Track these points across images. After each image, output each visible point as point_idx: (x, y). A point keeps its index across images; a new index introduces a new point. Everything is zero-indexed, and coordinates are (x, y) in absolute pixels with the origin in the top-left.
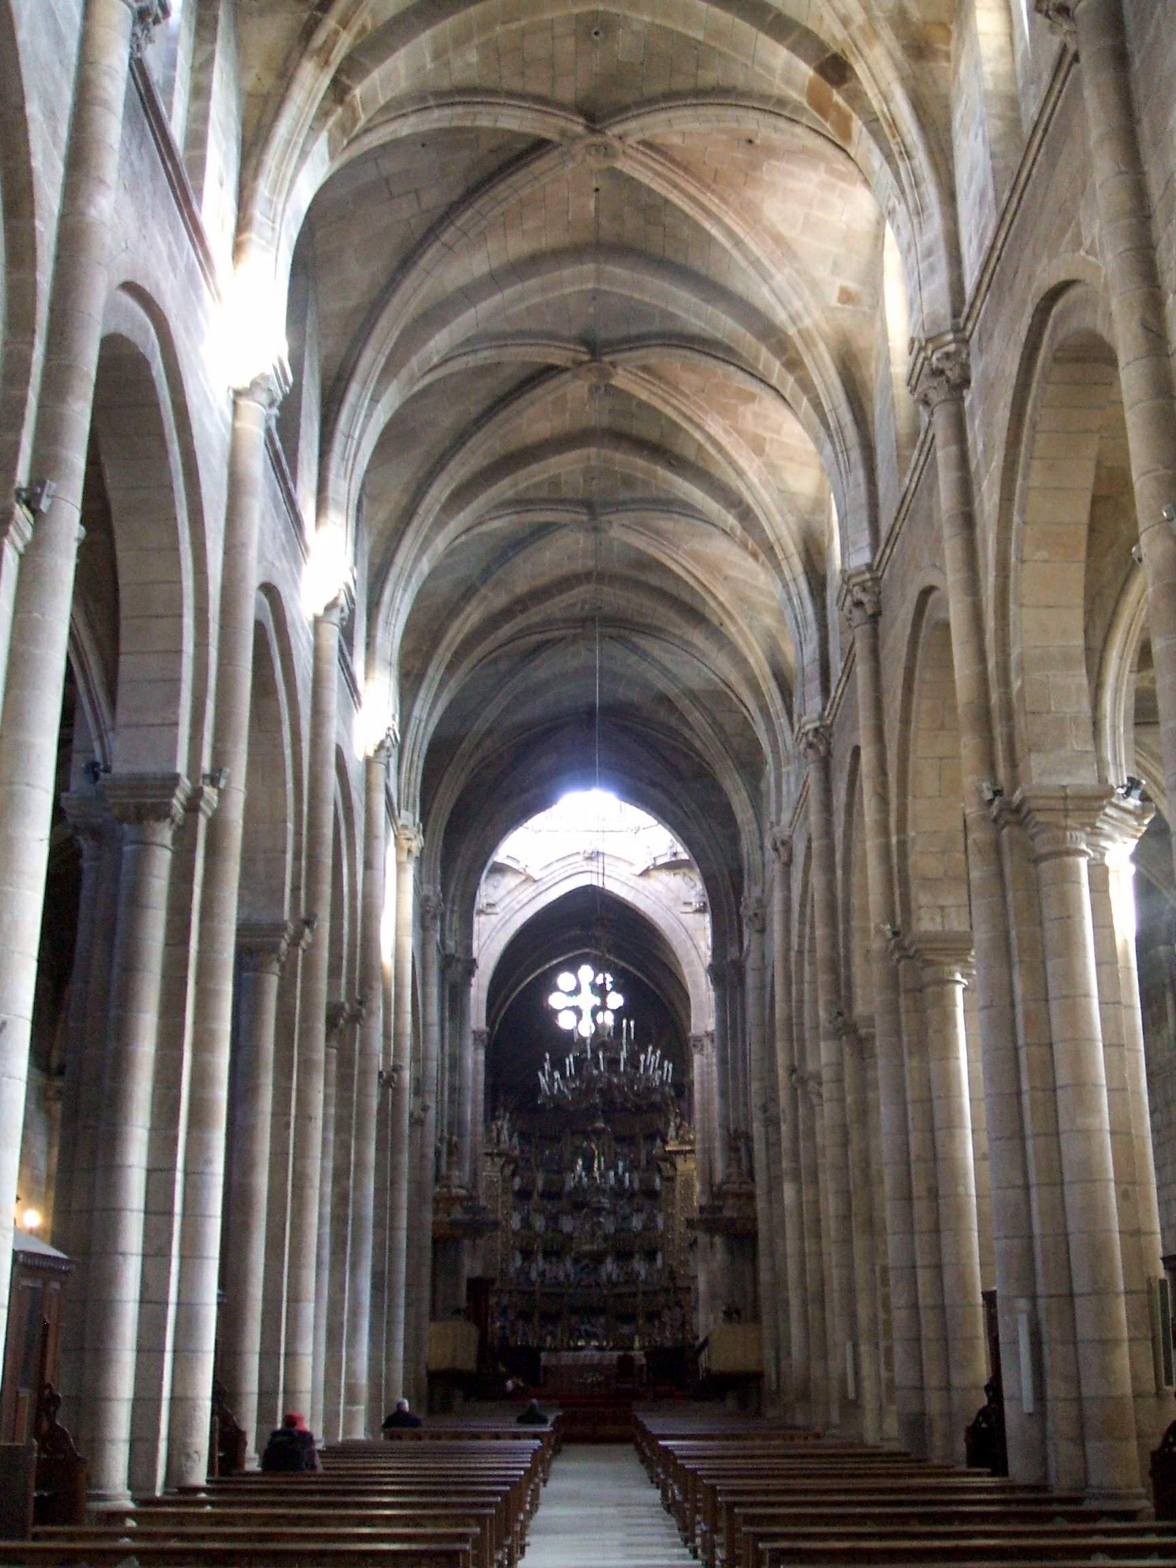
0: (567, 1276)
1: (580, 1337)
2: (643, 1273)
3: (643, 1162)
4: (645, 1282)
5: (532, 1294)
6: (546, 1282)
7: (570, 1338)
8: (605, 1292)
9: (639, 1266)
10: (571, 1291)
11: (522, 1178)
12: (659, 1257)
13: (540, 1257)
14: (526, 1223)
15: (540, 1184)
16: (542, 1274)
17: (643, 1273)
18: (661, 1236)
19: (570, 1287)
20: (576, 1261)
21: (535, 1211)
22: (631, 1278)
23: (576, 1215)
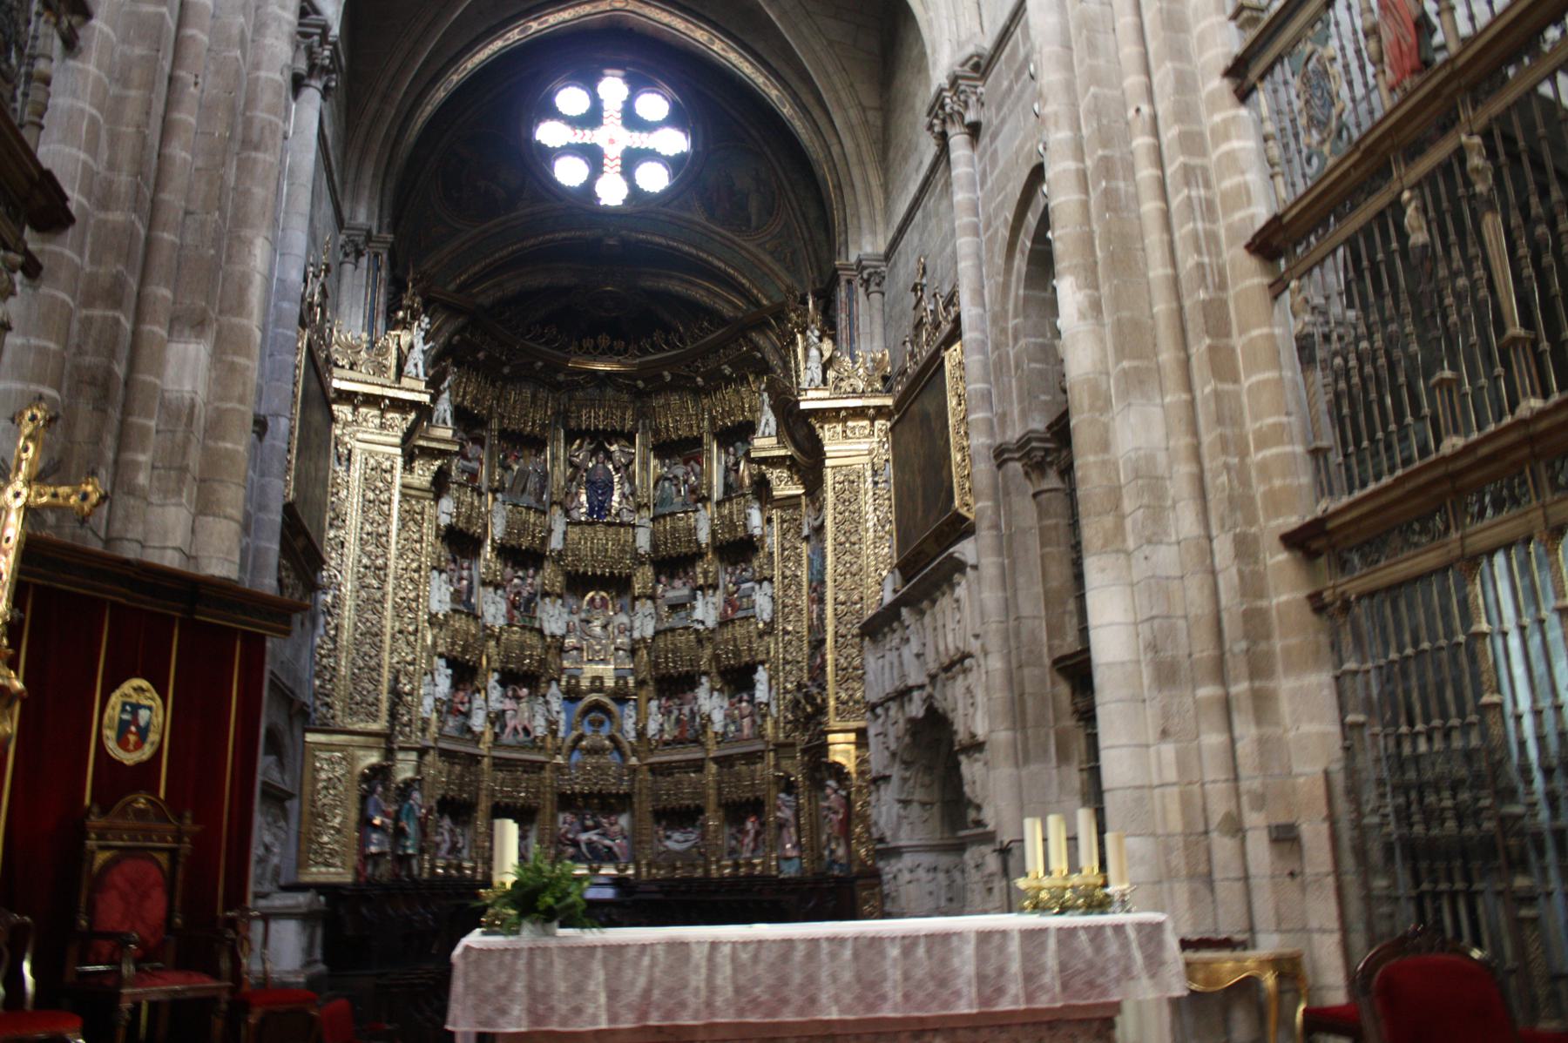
0: (552, 725)
1: (576, 859)
2: (718, 717)
4: (722, 738)
5: (474, 759)
6: (507, 738)
8: (633, 761)
9: (711, 703)
10: (559, 759)
11: (459, 504)
12: (761, 675)
14: (463, 603)
15: (497, 530)
16: (497, 718)
17: (718, 717)
18: (770, 628)
19: (558, 750)
20: (572, 695)
21: (484, 583)
22: (692, 731)
23: (571, 601)
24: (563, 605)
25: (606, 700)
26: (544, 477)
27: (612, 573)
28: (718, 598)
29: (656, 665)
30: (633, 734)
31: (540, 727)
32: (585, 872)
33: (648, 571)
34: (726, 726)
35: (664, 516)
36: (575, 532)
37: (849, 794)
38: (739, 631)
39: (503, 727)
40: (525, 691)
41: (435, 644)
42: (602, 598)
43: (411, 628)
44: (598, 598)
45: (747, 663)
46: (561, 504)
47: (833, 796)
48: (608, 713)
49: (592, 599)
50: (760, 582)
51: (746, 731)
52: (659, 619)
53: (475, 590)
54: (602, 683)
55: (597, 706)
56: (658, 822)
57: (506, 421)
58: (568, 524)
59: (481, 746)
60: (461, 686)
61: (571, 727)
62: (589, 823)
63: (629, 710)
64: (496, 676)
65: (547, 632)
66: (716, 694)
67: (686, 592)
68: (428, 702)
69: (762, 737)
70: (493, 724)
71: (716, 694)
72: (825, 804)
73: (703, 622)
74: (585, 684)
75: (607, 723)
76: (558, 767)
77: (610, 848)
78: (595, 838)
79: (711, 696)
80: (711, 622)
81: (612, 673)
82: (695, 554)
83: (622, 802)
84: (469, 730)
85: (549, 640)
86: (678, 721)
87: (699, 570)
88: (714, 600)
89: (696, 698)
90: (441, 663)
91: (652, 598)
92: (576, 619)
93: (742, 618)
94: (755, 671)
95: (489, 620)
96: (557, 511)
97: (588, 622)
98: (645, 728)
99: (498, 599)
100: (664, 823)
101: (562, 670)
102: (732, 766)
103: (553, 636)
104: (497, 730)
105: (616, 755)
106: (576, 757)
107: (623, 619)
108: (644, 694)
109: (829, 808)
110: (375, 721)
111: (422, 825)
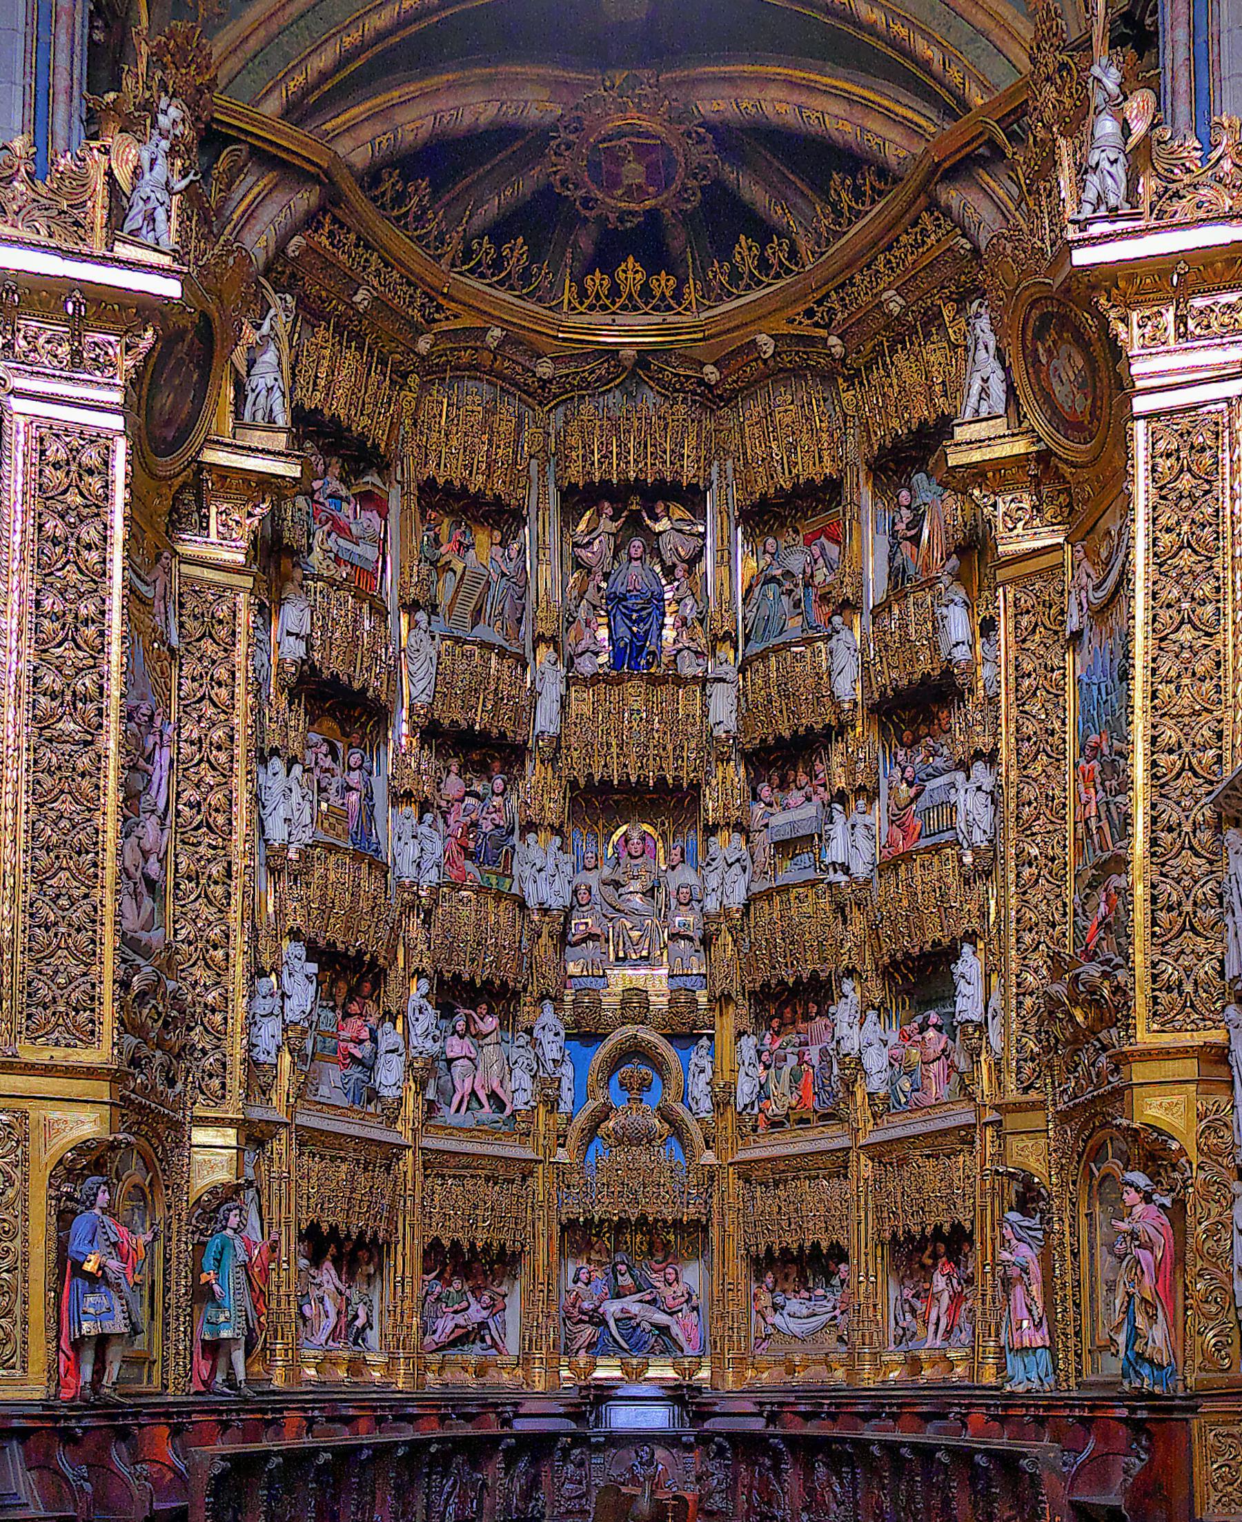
4: (882, 1107)
8: (709, 1157)
12: (970, 964)
13: (418, 989)
17: (875, 1060)
19: (561, 1139)
21: (399, 798)
25: (648, 1035)
26: (520, 584)
30: (706, 1104)
32: (618, 1373)
33: (735, 774)
34: (892, 1083)
35: (763, 656)
36: (582, 703)
40: (491, 1023)
42: (644, 837)
43: (216, 870)
44: (635, 835)
46: (553, 641)
48: (659, 1066)
49: (626, 838)
50: (964, 766)
53: (378, 812)
55: (634, 1052)
56: (759, 1278)
57: (432, 465)
59: (399, 1127)
60: (354, 1008)
62: (626, 1280)
63: (699, 1057)
64: (424, 985)
65: (531, 903)
66: (872, 1015)
67: (811, 810)
70: (422, 1085)
71: (872, 1015)
72: (1124, 1226)
75: (657, 1081)
76: (561, 1171)
77: (664, 1330)
78: (635, 1309)
80: (860, 869)
82: (828, 727)
87: (836, 759)
88: (868, 819)
91: (741, 828)
92: (592, 879)
93: (927, 850)
94: (952, 954)
96: (545, 654)
97: (617, 885)
98: (730, 1089)
100: (769, 1279)
103: (545, 911)
104: (431, 1094)
107: (686, 876)
108: (726, 1024)
109: (1133, 1235)
110: (88, 1044)
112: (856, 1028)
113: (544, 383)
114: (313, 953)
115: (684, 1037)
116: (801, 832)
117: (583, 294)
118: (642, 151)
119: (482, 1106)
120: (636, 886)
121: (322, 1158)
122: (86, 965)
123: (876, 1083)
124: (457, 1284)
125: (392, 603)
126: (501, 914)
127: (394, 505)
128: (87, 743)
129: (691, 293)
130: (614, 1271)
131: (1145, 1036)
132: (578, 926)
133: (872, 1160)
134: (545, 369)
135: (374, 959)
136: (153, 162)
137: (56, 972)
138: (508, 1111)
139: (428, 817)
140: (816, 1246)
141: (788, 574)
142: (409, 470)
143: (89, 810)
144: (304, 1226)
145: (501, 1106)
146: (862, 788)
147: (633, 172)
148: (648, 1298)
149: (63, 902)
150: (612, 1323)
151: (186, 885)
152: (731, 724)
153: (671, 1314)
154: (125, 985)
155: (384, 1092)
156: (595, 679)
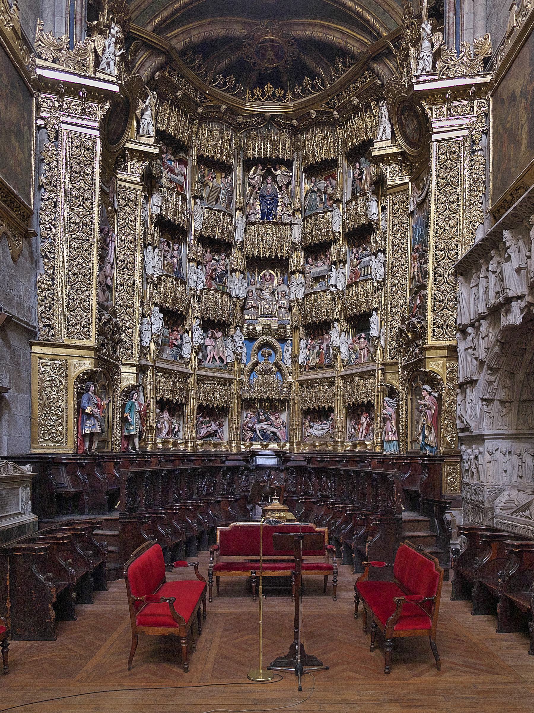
2: (344, 349)
3: (347, 196)
4: (347, 363)
5: (186, 376)
7: (243, 439)
8: (290, 379)
12: (375, 318)
13: (196, 323)
17: (344, 349)
19: (242, 372)
24: (244, 278)
26: (231, 191)
27: (276, 256)
28: (347, 269)
29: (305, 316)
30: (290, 361)
31: (229, 357)
32: (260, 447)
33: (300, 255)
34: (349, 355)
35: (310, 216)
36: (251, 230)
37: (440, 396)
38: (360, 289)
39: (205, 357)
40: (220, 334)
41: (151, 297)
42: (271, 275)
43: (130, 283)
45: (364, 311)
46: (241, 210)
47: (427, 397)
48: (274, 348)
49: (264, 275)
50: (375, 254)
51: (363, 358)
52: (308, 287)
53: (183, 265)
54: (270, 329)
55: (267, 344)
56: (305, 418)
57: (202, 150)
58: (247, 223)
59: (189, 367)
60: (175, 328)
61: (249, 358)
62: (262, 417)
63: (287, 346)
64: (198, 321)
66: (343, 334)
67: (325, 267)
68: (147, 336)
69: (374, 361)
70: (197, 354)
71: (343, 334)
72: (422, 402)
73: (336, 287)
74: (259, 328)
75: (273, 354)
76: (242, 383)
77: (275, 433)
78: (265, 427)
79: (340, 336)
80: (340, 287)
81: (276, 323)
82: (331, 240)
83: (284, 404)
84: (181, 357)
85: (235, 300)
86: (318, 353)
87: (333, 251)
88: (343, 271)
89: (330, 338)
90: (157, 309)
91: (303, 273)
92: (253, 288)
93: (362, 281)
94: (370, 315)
95: (193, 284)
96: (239, 214)
97: (261, 290)
98: (297, 357)
99: (199, 271)
100: (309, 418)
101: (244, 321)
102: (353, 381)
103: (238, 298)
104: (200, 357)
105: (279, 375)
106: (254, 377)
107: (284, 288)
108: (296, 336)
109: (425, 405)
110: (87, 339)
111: (143, 417)
112: (338, 338)
113: (240, 124)
114: (162, 310)
115: (282, 340)
116: (321, 274)
117: (253, 95)
118: (273, 47)
119: (216, 361)
120: (268, 291)
121: (164, 377)
122: (87, 313)
123: (344, 356)
124: (208, 418)
125: (188, 196)
126: (223, 299)
127: (189, 163)
128: (87, 240)
129: (289, 96)
130: (259, 415)
131: (431, 342)
132: (249, 303)
133: (342, 380)
134: (240, 119)
135: (182, 313)
136: (109, 45)
137: (77, 315)
138: (225, 363)
139: (200, 267)
140: (324, 407)
141: (319, 190)
142: (194, 152)
143: (88, 262)
144: (158, 399)
145: (223, 361)
146: (342, 261)
147: (270, 54)
148: (270, 423)
149: (79, 292)
150: (258, 431)
151: (120, 287)
152: (300, 239)
153: (277, 428)
154: (99, 320)
155: (185, 356)
156: (255, 223)
